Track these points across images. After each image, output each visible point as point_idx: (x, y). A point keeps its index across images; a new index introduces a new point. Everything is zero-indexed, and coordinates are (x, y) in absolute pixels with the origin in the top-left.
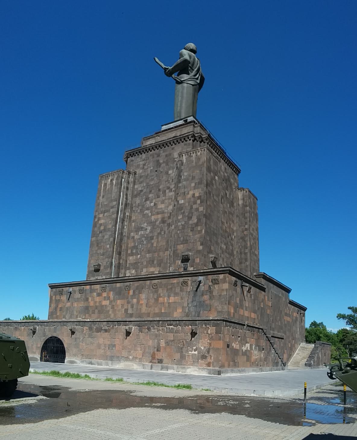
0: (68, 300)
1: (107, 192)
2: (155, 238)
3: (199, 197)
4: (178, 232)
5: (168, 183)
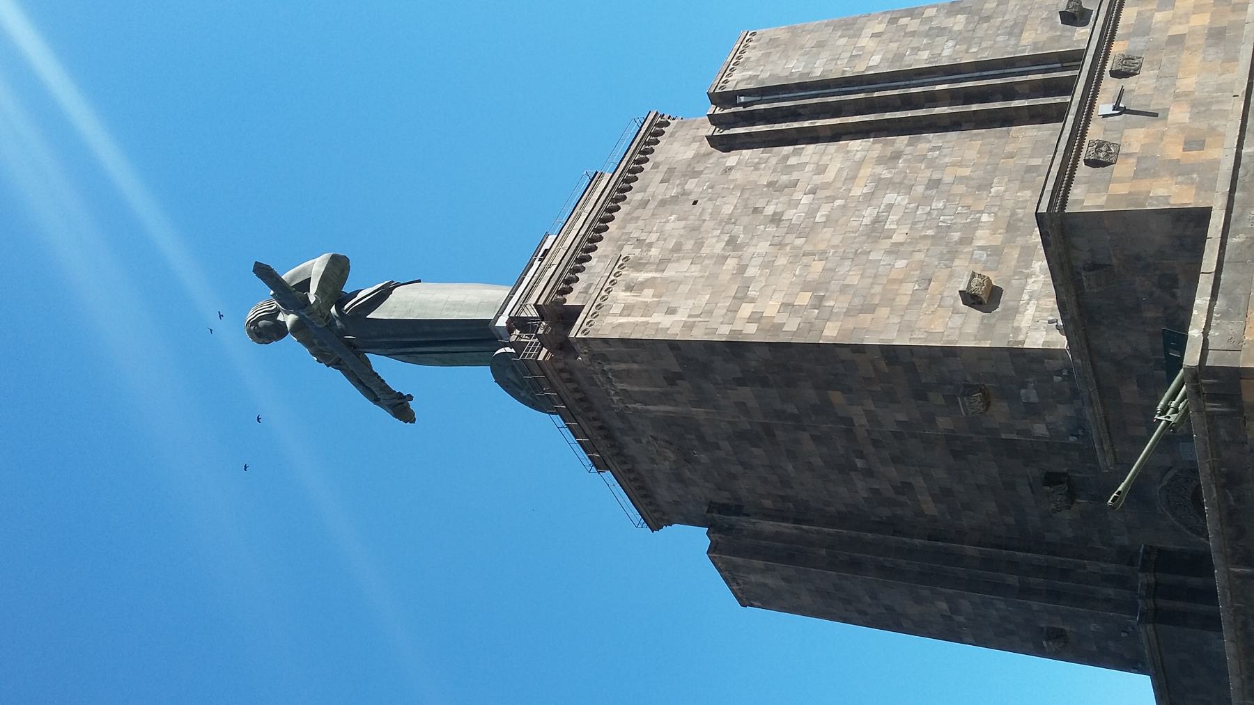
0: (1156, 115)
2: (935, 176)
3: (893, 21)
4: (974, 50)
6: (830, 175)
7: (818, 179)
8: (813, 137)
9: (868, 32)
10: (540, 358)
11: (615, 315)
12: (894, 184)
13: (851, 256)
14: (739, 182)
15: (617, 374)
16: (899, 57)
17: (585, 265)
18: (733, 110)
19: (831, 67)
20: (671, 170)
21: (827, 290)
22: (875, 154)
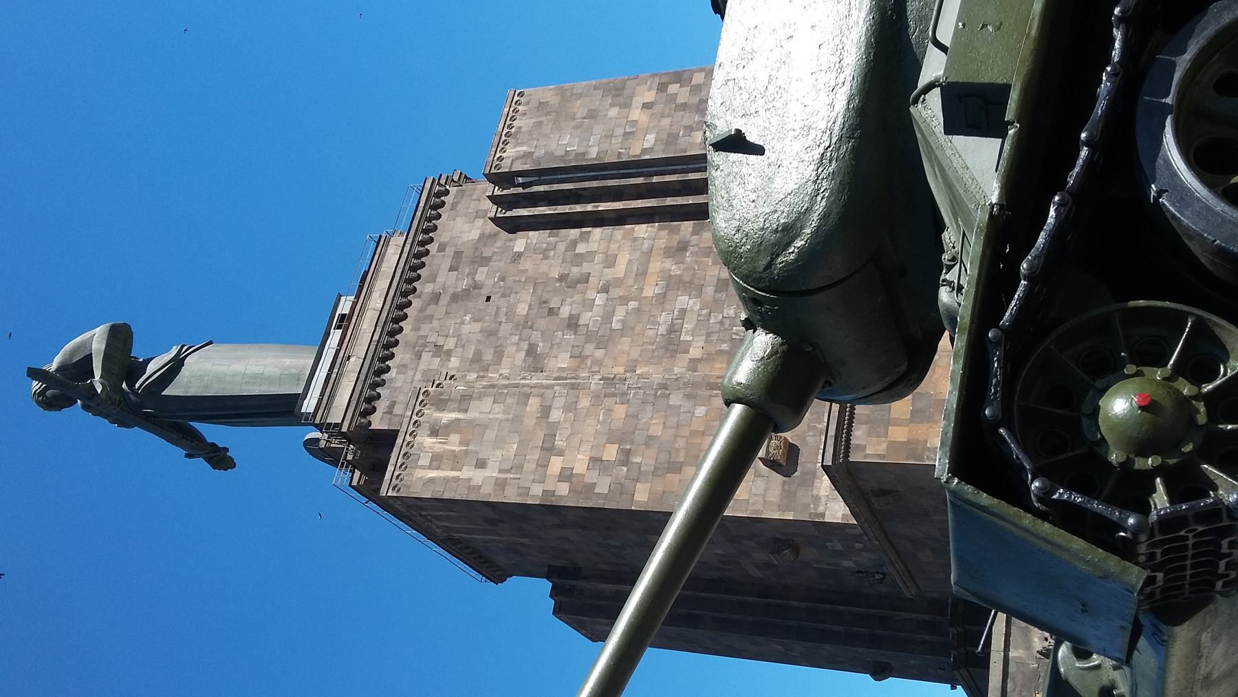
1: (471, 448)
3: (662, 88)
5: (555, 248)
6: (620, 269)
7: (609, 274)
8: (599, 220)
9: (638, 101)
10: (355, 483)
11: (423, 467)
12: (684, 283)
13: (651, 399)
14: (530, 273)
15: (437, 518)
16: (672, 138)
17: (384, 377)
18: (512, 191)
19: (605, 146)
20: (458, 254)
21: (632, 442)
22: (661, 243)
